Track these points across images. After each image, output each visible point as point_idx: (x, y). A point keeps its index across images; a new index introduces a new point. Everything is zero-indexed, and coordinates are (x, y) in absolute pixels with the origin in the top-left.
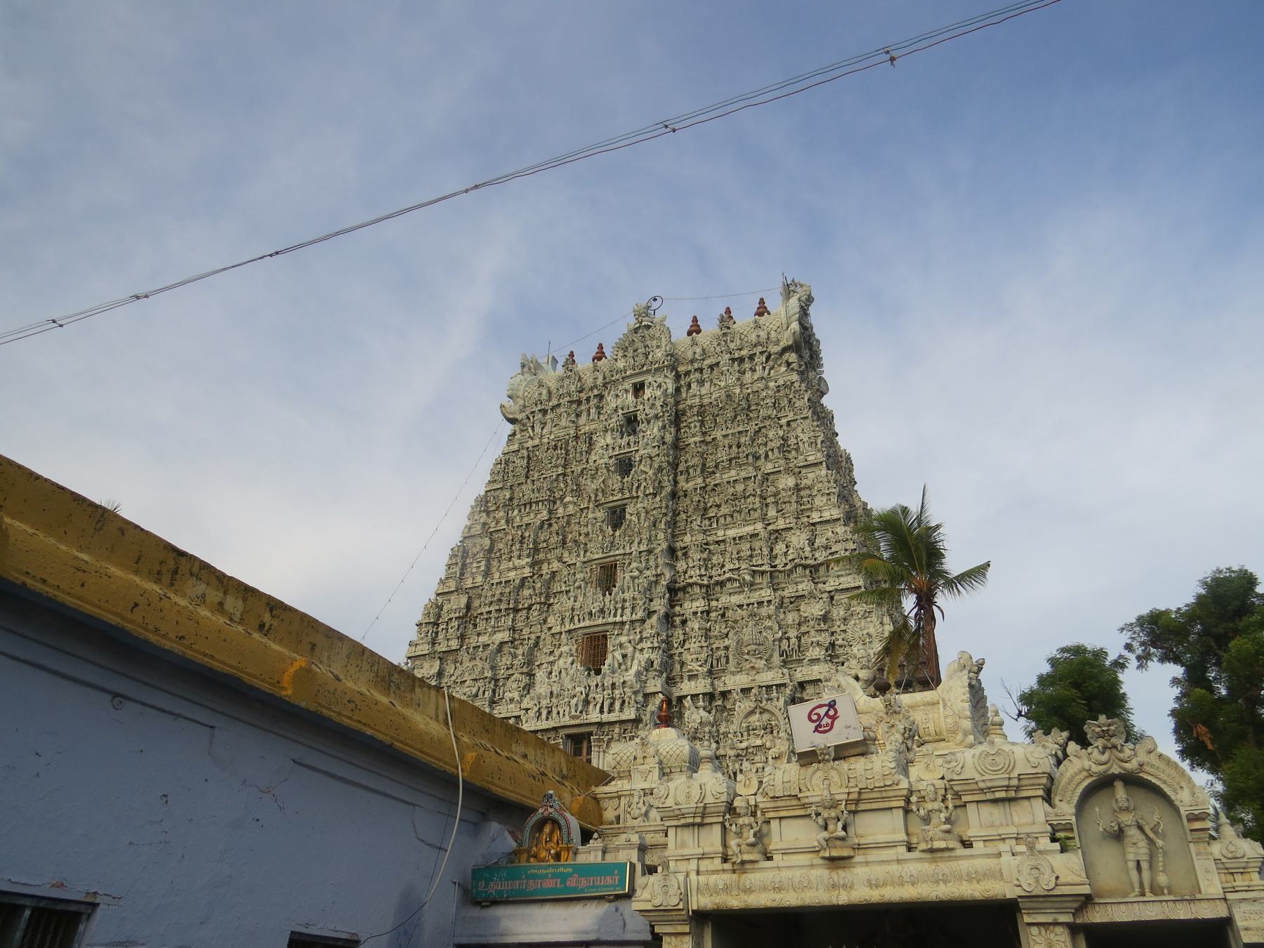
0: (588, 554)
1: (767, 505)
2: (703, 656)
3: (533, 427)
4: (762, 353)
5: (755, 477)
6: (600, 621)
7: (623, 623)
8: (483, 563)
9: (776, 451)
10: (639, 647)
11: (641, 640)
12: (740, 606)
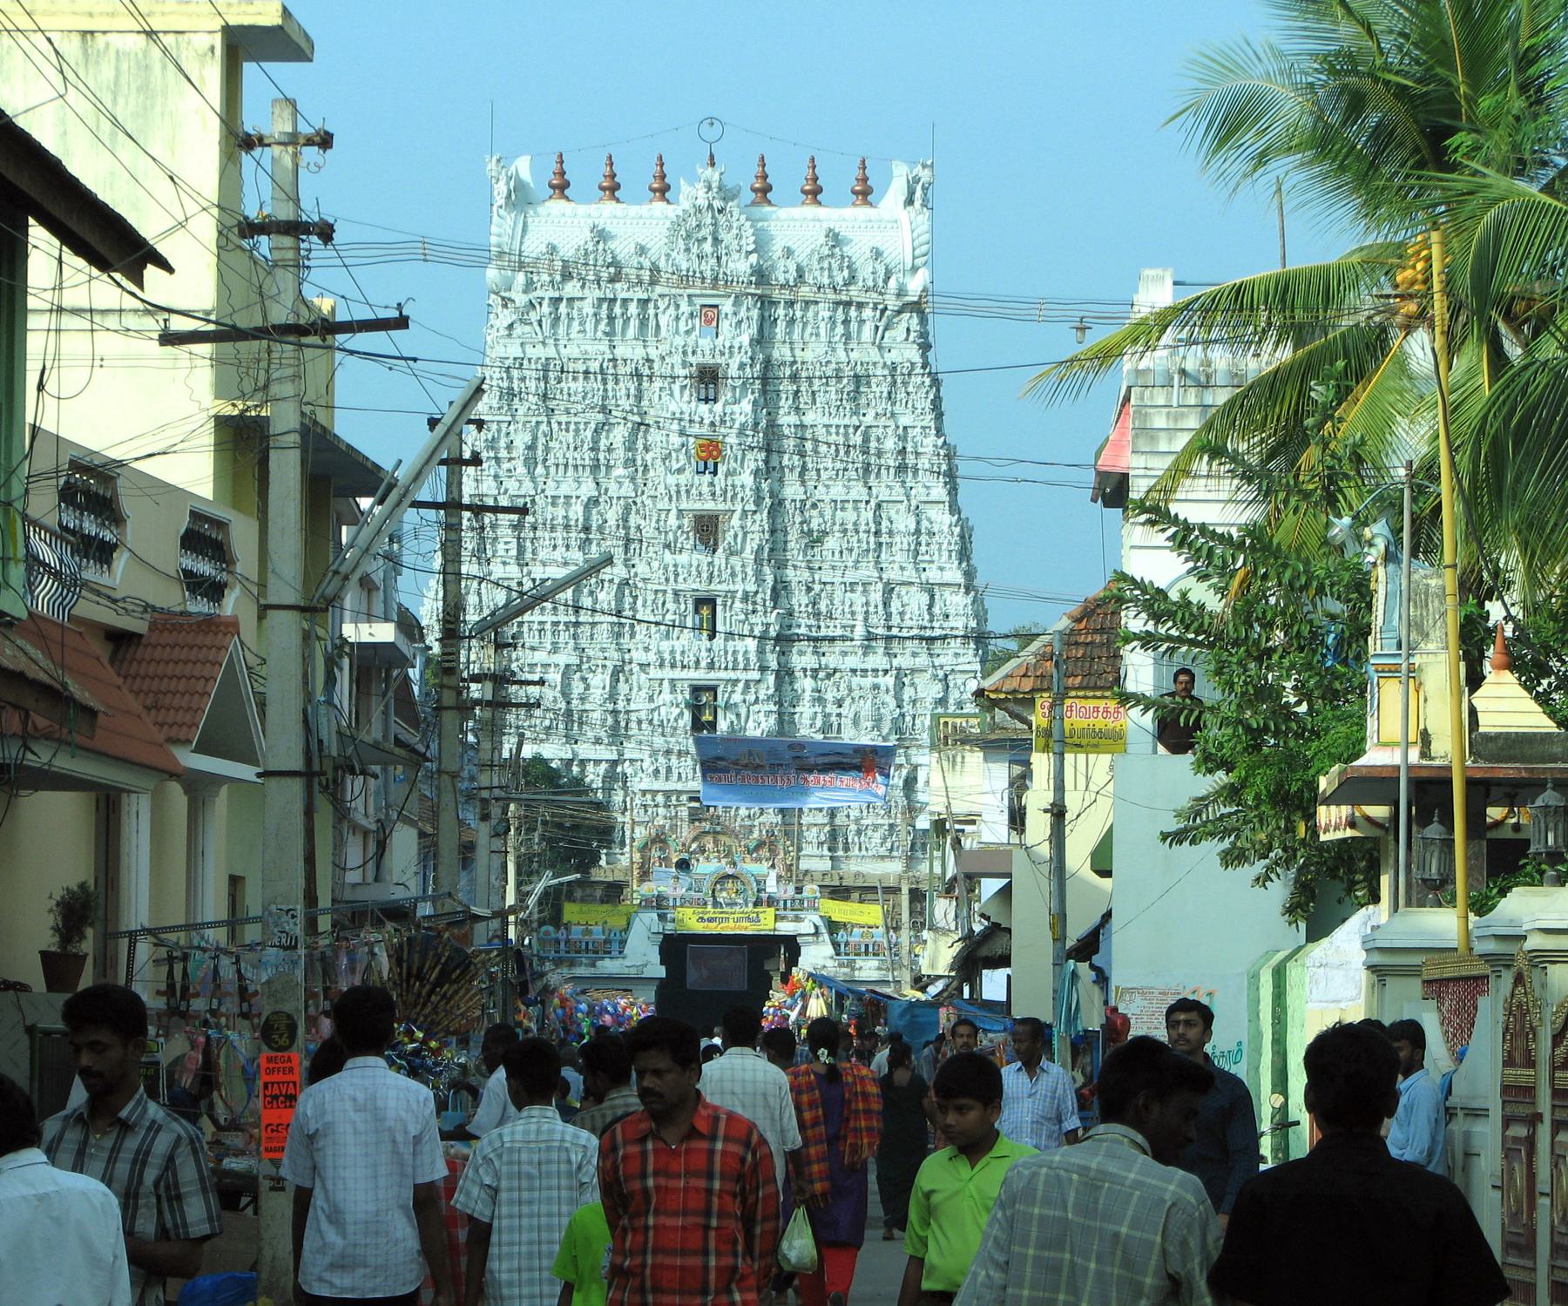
0: (680, 579)
1: (880, 544)
2: (819, 723)
3: (540, 323)
4: (875, 305)
5: (867, 502)
6: (712, 675)
7: (738, 681)
8: (514, 545)
9: (892, 471)
10: (756, 708)
11: (757, 701)
12: (854, 671)
